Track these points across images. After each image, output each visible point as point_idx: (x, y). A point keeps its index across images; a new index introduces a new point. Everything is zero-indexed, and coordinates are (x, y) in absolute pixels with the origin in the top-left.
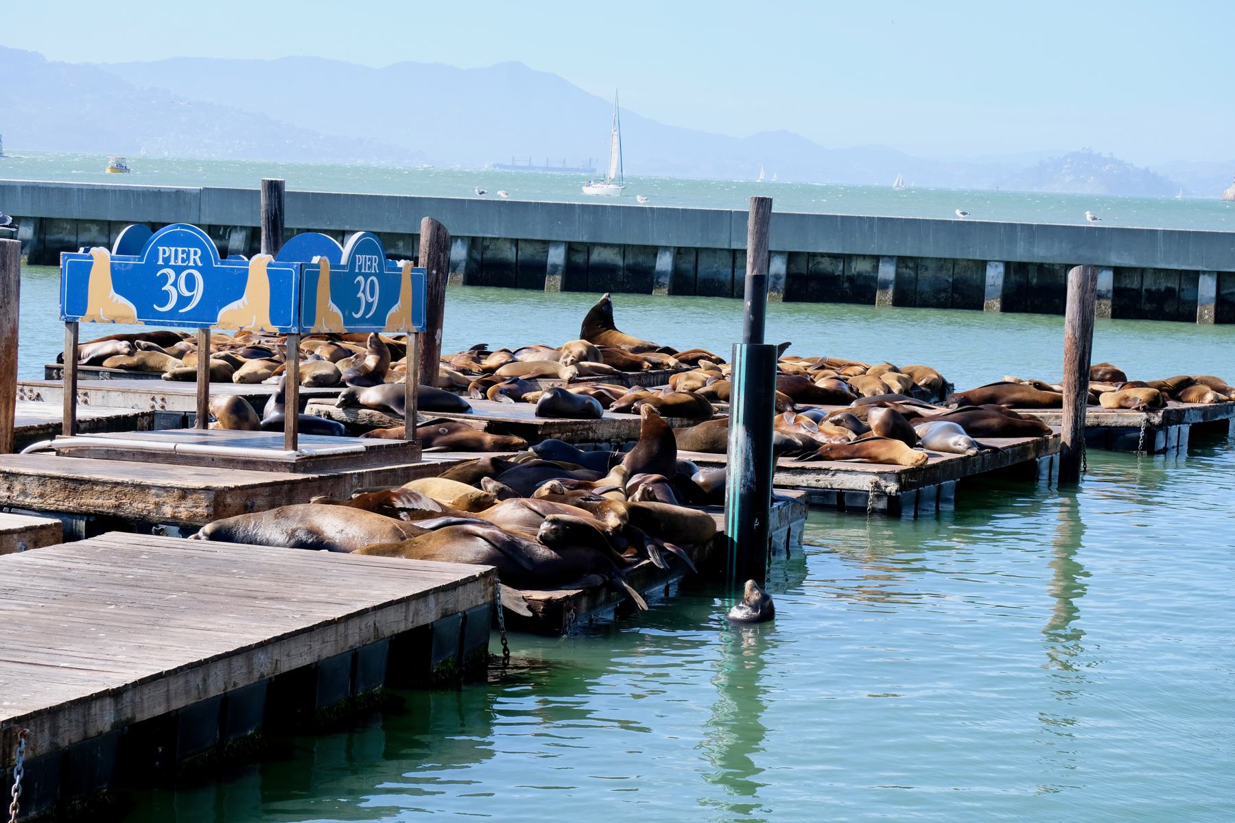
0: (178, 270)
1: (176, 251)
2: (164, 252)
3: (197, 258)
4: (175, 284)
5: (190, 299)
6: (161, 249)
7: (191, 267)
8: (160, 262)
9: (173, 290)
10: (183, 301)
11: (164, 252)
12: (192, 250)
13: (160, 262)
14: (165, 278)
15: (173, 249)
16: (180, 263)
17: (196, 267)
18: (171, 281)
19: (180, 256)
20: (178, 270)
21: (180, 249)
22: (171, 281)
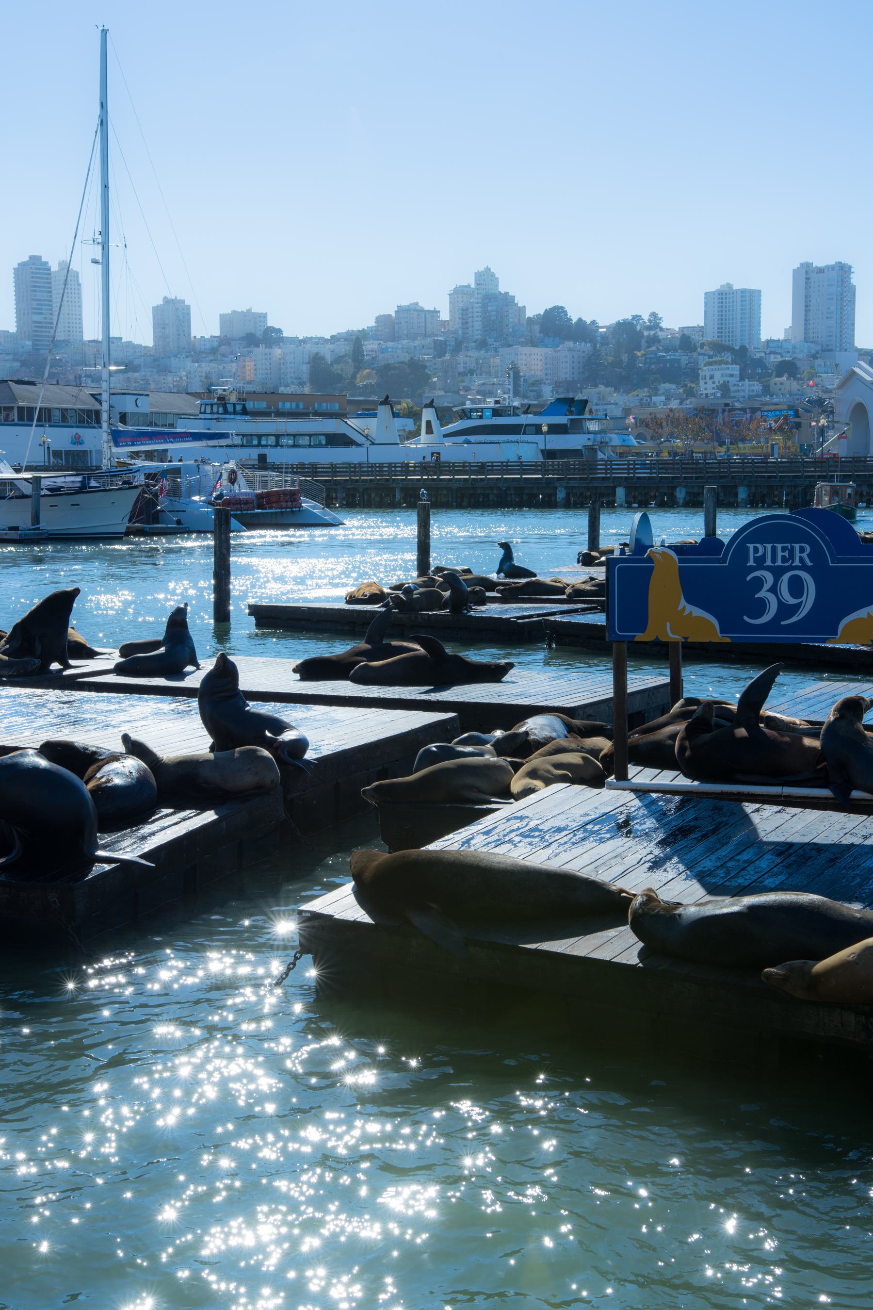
0: (777, 573)
1: (774, 550)
2: (756, 550)
3: (805, 555)
4: (773, 590)
5: (797, 607)
6: (751, 546)
7: (797, 568)
8: (751, 563)
9: (771, 597)
10: (785, 611)
11: (756, 550)
12: (797, 546)
13: (751, 563)
14: (758, 583)
15: (769, 546)
16: (779, 563)
17: (804, 567)
18: (768, 585)
19: (780, 554)
20: (777, 573)
21: (779, 546)
22: (768, 585)
